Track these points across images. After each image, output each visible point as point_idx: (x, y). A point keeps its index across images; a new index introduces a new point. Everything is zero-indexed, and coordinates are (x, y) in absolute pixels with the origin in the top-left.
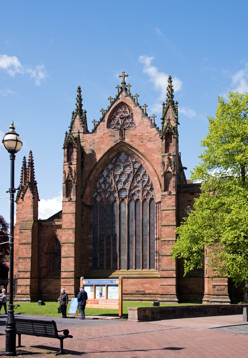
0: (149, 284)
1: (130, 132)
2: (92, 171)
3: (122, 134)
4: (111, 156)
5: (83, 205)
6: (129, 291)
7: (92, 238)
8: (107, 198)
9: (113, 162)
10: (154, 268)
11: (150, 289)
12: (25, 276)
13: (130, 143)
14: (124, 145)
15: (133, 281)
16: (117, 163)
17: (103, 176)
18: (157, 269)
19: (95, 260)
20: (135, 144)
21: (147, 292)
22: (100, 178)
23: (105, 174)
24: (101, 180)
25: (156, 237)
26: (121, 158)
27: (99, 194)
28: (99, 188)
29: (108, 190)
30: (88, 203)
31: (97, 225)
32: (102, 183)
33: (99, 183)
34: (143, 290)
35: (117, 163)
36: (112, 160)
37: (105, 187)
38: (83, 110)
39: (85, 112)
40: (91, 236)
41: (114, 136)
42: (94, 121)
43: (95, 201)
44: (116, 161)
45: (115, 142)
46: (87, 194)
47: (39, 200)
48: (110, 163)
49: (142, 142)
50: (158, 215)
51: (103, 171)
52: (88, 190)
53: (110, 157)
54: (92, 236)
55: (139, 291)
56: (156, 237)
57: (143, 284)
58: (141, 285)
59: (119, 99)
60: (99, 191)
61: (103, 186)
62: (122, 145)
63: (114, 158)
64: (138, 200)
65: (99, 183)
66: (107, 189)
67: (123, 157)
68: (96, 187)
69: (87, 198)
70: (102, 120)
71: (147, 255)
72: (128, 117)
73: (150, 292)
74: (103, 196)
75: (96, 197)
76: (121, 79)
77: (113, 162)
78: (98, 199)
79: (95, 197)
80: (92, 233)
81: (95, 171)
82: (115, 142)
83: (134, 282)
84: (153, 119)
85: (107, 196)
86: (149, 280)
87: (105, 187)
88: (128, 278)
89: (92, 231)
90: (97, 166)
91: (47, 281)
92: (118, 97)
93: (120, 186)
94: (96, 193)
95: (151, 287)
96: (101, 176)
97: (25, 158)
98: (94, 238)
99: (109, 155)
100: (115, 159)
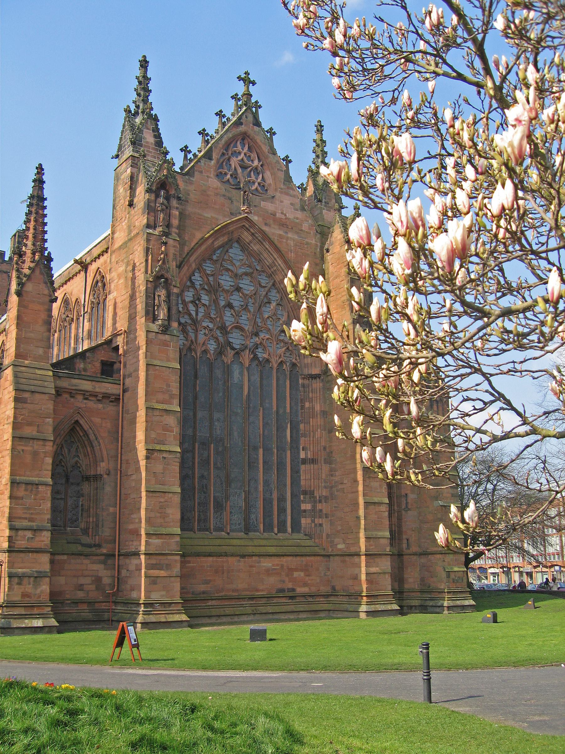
0: (301, 570)
1: (263, 204)
6: (263, 590)
11: (305, 585)
12: (35, 544)
14: (247, 226)
21: (301, 590)
34: (290, 586)
55: (281, 590)
57: (291, 570)
58: (287, 575)
63: (219, 247)
73: (305, 590)
77: (215, 258)
83: (273, 565)
88: (259, 556)
95: (307, 578)
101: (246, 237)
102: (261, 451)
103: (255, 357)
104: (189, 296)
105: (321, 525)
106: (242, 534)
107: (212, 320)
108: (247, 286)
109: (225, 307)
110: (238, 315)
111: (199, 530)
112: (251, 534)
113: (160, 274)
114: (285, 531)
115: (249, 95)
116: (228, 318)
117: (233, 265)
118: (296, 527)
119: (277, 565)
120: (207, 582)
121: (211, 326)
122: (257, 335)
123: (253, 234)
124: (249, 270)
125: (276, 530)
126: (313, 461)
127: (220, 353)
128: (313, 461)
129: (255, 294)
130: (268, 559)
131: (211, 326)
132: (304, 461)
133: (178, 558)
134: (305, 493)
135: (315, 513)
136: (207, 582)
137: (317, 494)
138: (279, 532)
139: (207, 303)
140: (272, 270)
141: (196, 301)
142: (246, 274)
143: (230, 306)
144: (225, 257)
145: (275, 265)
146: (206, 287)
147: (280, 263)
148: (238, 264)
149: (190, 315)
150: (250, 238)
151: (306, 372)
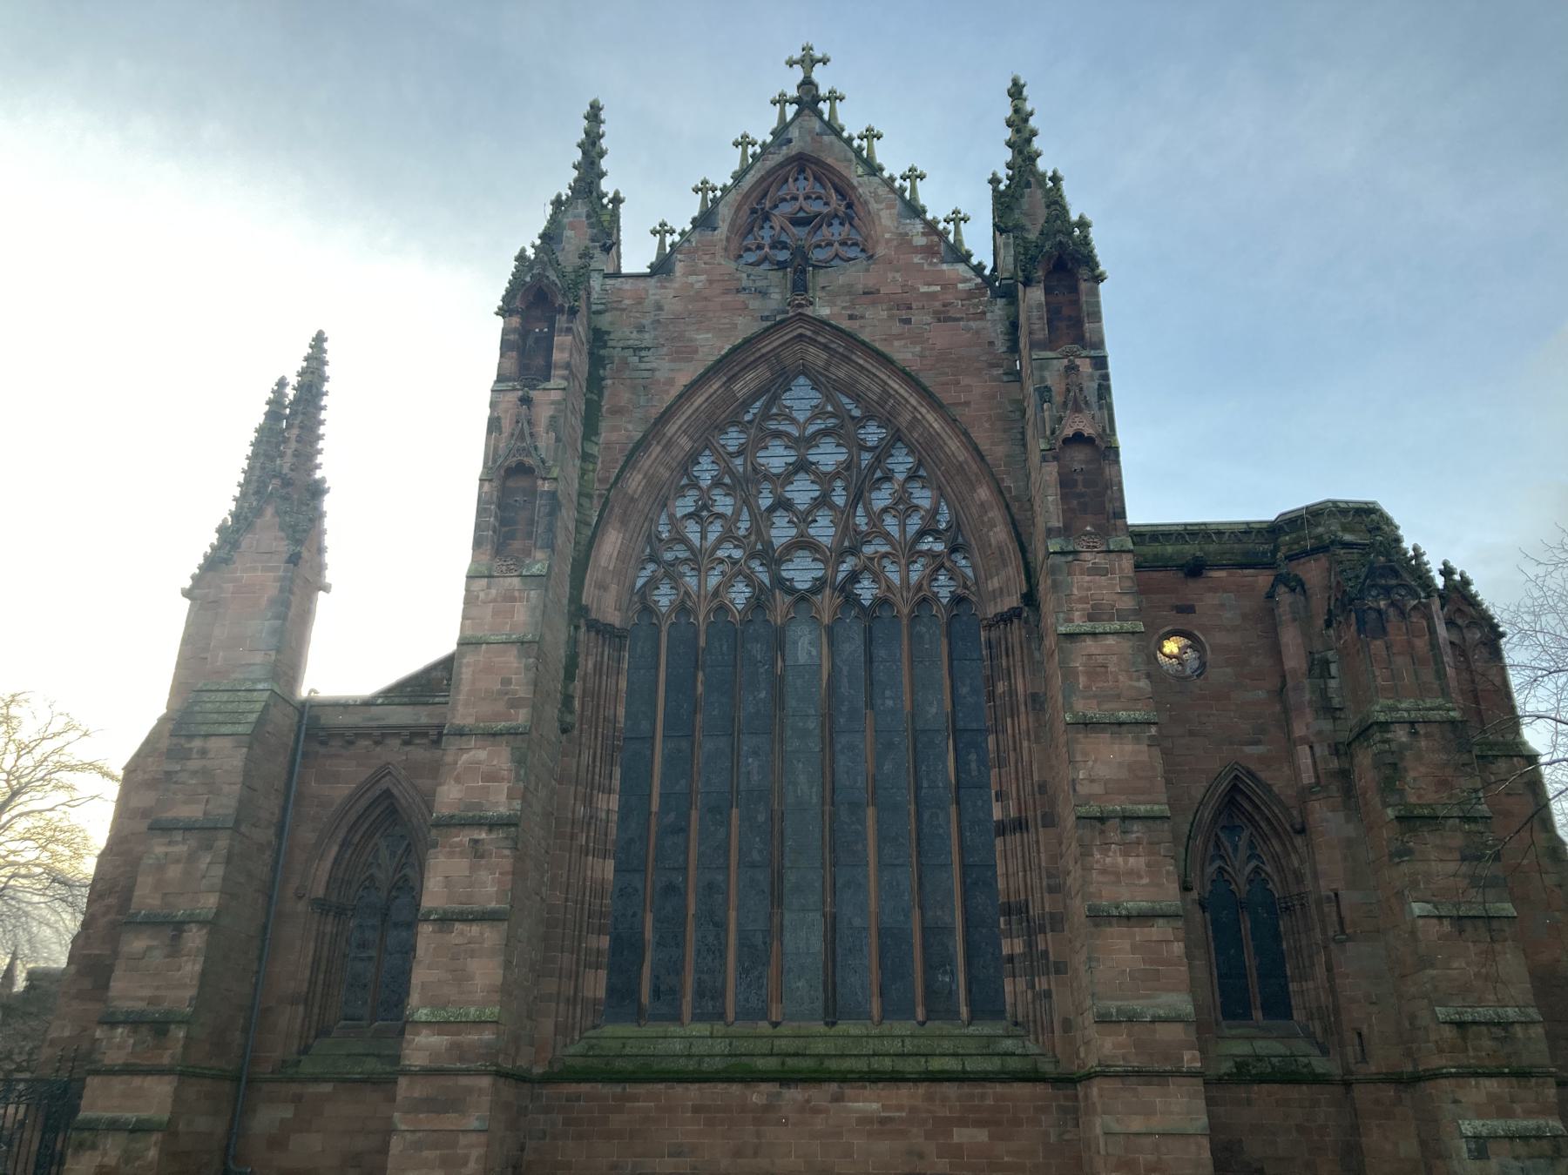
0: (979, 1123)
2: (641, 446)
3: (800, 286)
4: (741, 388)
5: (582, 622)
7: (615, 817)
8: (716, 593)
9: (747, 417)
10: (998, 1014)
13: (845, 324)
14: (809, 333)
15: (875, 1106)
16: (772, 425)
17: (694, 484)
18: (1016, 1024)
19: (626, 951)
20: (874, 326)
22: (681, 492)
23: (708, 476)
24: (685, 505)
25: (997, 814)
26: (788, 399)
27: (671, 572)
28: (671, 540)
29: (720, 554)
30: (614, 618)
31: (653, 738)
32: (689, 516)
33: (671, 517)
35: (772, 425)
36: (745, 405)
37: (703, 537)
38: (605, 195)
39: (617, 200)
40: (609, 804)
41: (763, 293)
42: (662, 230)
43: (648, 609)
44: (766, 415)
45: (763, 318)
46: (603, 562)
47: (326, 588)
48: (733, 423)
49: (908, 321)
50: (1001, 687)
51: (693, 458)
52: (612, 543)
53: (736, 388)
54: (614, 802)
56: (997, 814)
59: (790, 141)
60: (669, 556)
61: (692, 531)
62: (801, 335)
63: (755, 397)
64: (882, 602)
65: (671, 517)
66: (717, 547)
67: (801, 399)
68: (653, 538)
69: (602, 587)
70: (704, 221)
71: (952, 930)
72: (829, 219)
74: (691, 581)
75: (653, 583)
76: (798, 74)
78: (664, 598)
79: (645, 585)
80: (616, 783)
81: (656, 450)
82: (763, 318)
84: (951, 227)
85: (713, 581)
86: (983, 1097)
87: (703, 537)
89: (617, 772)
90: (671, 429)
91: (298, 1099)
92: (781, 133)
93: (782, 531)
94: (651, 567)
96: (684, 481)
97: (282, 383)
98: (625, 812)
99: (732, 379)
100: (758, 404)
101: (816, 356)
102: (871, 811)
103: (851, 600)
104: (685, 505)
105: (1048, 994)
106: (820, 1027)
107: (739, 543)
108: (828, 456)
109: (771, 510)
110: (806, 518)
111: (698, 1018)
112: (842, 1027)
113: (512, 461)
114: (953, 1015)
115: (807, 84)
116: (782, 531)
117: (793, 421)
118: (986, 1005)
119: (900, 1108)
120: (677, 1153)
121: (737, 554)
122: (854, 551)
123: (826, 347)
124: (831, 422)
125: (920, 1013)
126: (1020, 825)
127: (759, 603)
128: (1020, 825)
129: (848, 468)
130: (870, 1090)
131: (737, 554)
132: (1002, 829)
133: (485, 1082)
134: (1008, 910)
135: (1037, 963)
136: (677, 1153)
137: (1034, 911)
138: (928, 1018)
139: (729, 511)
140: (887, 407)
142: (826, 433)
143: (783, 504)
144: (774, 410)
145: (890, 396)
146: (727, 480)
147: (896, 386)
148: (801, 417)
149: (683, 540)
150: (824, 356)
151: (992, 610)
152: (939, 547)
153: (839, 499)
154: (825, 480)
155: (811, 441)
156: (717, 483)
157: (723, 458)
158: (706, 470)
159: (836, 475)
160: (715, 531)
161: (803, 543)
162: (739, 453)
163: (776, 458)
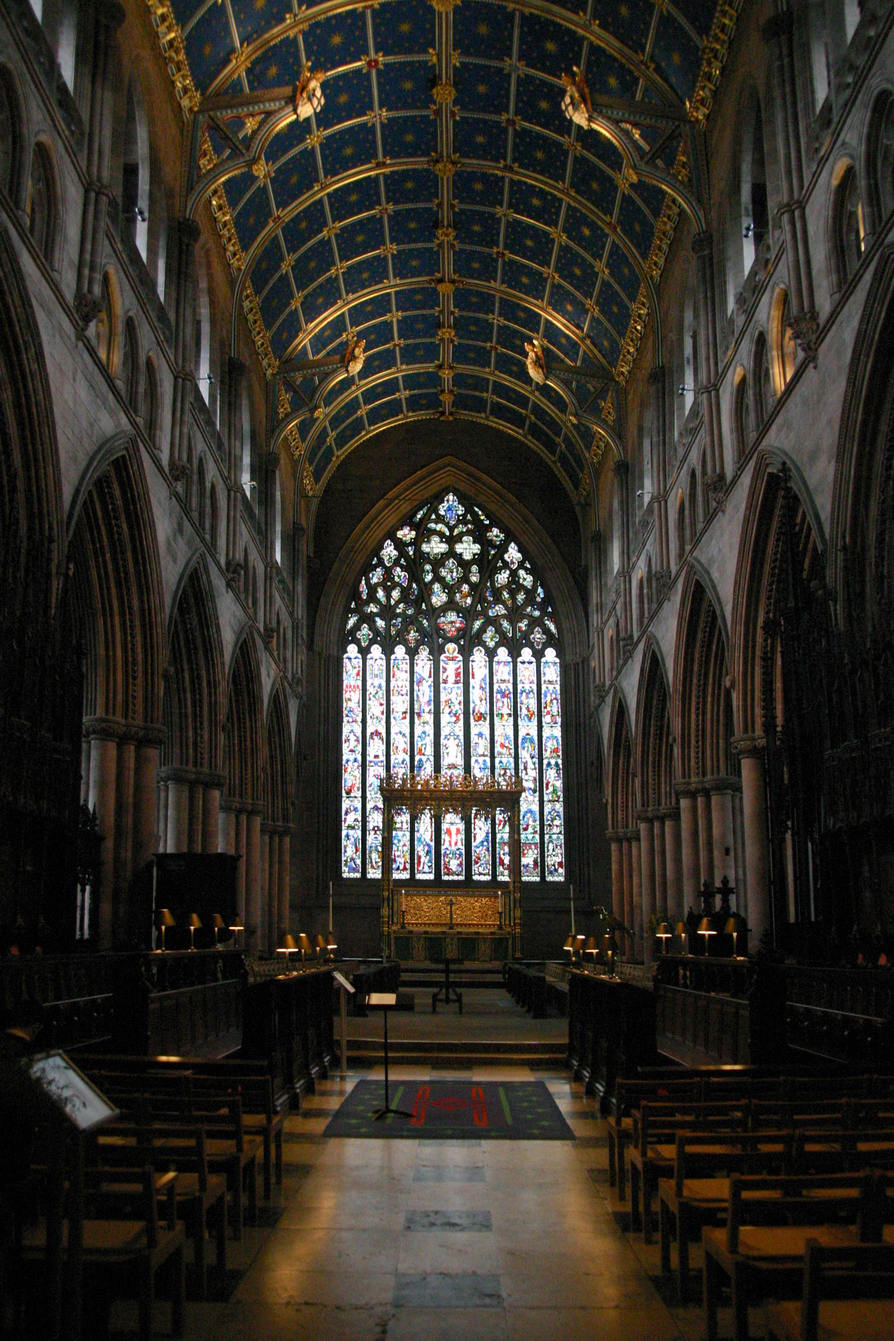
17: (381, 563)
24: (376, 577)
51: (382, 548)
61: (381, 594)
67: (450, 504)
68: (356, 595)
75: (357, 627)
87: (388, 597)
109: (432, 582)
141: (388, 583)
149: (377, 601)
152: (537, 613)
153: (474, 579)
154: (464, 565)
155: (459, 539)
156: (396, 563)
157: (400, 545)
158: (389, 551)
159: (473, 562)
160: (396, 594)
161: (451, 605)
162: (411, 544)
163: (435, 547)
